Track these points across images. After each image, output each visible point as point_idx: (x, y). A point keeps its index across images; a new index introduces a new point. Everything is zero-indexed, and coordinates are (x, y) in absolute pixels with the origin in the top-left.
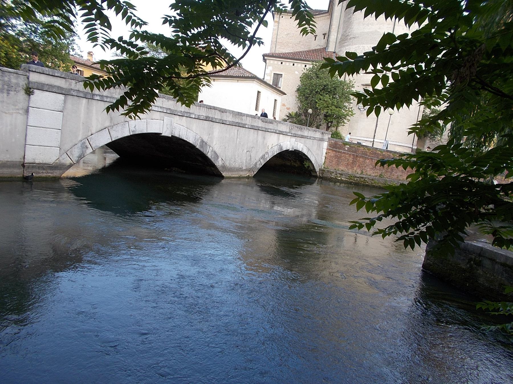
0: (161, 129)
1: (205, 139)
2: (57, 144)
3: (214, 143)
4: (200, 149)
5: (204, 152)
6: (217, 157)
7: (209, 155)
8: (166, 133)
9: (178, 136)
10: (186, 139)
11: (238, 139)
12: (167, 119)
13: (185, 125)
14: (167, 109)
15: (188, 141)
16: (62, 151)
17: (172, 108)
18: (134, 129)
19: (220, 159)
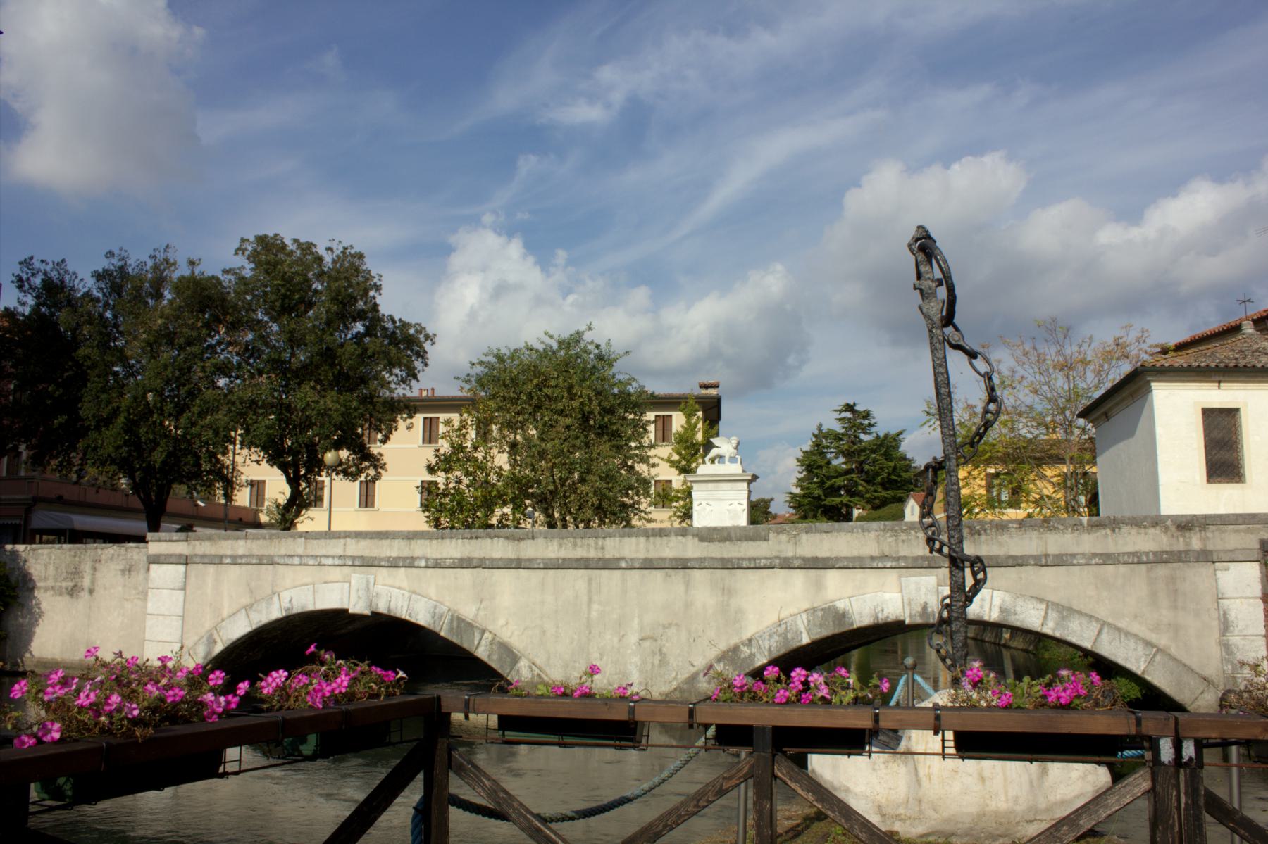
0: (346, 600)
1: (468, 611)
2: (177, 637)
3: (502, 622)
4: (449, 638)
5: (465, 646)
6: (513, 657)
7: (482, 653)
8: (357, 606)
9: (385, 612)
10: (408, 618)
11: (595, 606)
12: (358, 578)
13: (405, 584)
14: (354, 558)
15: (413, 620)
16: (185, 650)
17: (367, 554)
18: (288, 605)
19: (523, 664)
